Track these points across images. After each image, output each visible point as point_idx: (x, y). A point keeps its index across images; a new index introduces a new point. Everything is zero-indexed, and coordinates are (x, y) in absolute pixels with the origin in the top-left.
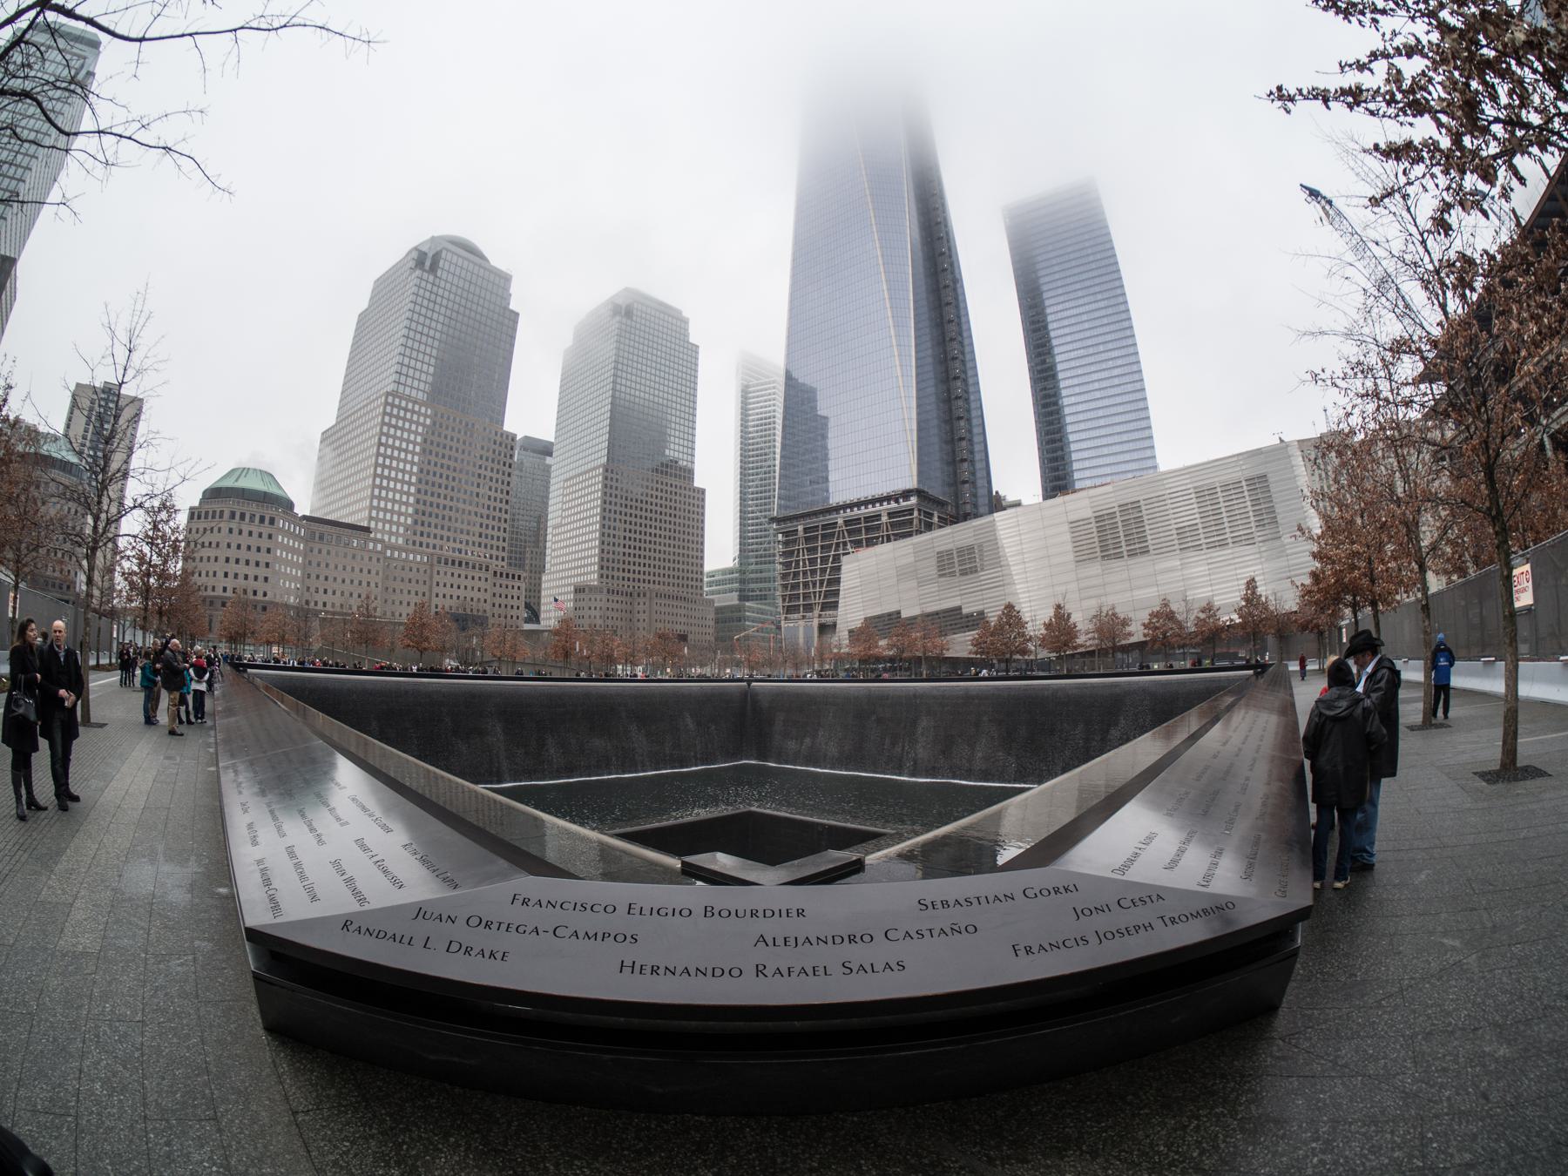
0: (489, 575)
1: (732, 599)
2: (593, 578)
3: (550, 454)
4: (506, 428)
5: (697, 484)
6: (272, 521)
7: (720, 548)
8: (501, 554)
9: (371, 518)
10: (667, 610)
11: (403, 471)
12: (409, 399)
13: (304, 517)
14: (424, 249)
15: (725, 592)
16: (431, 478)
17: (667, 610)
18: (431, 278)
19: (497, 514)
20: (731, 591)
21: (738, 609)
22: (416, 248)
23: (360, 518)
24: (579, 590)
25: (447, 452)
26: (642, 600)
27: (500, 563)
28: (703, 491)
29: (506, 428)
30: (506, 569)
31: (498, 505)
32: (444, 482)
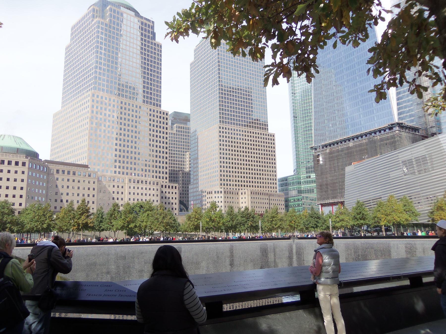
0: (159, 187)
3: (189, 121)
7: (285, 165)
8: (165, 176)
10: (258, 201)
13: (46, 161)
16: (122, 137)
17: (258, 201)
19: (161, 155)
23: (84, 162)
25: (130, 123)
26: (243, 196)
27: (165, 180)
28: (273, 136)
30: (168, 184)
31: (162, 150)
32: (130, 138)
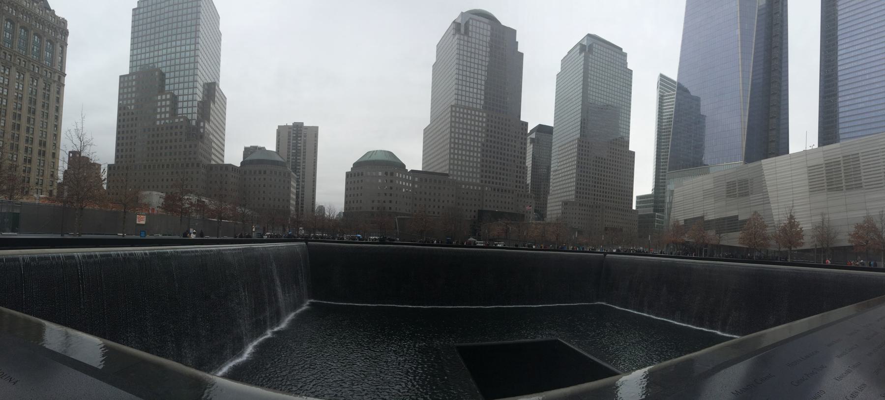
1: (650, 211)
2: (572, 198)
4: (522, 119)
5: (631, 148)
6: (392, 174)
9: (450, 169)
11: (466, 145)
12: (472, 109)
14: (459, 21)
15: (646, 207)
18: (466, 38)
20: (650, 206)
21: (653, 216)
22: (454, 22)
24: (565, 203)
29: (522, 119)
